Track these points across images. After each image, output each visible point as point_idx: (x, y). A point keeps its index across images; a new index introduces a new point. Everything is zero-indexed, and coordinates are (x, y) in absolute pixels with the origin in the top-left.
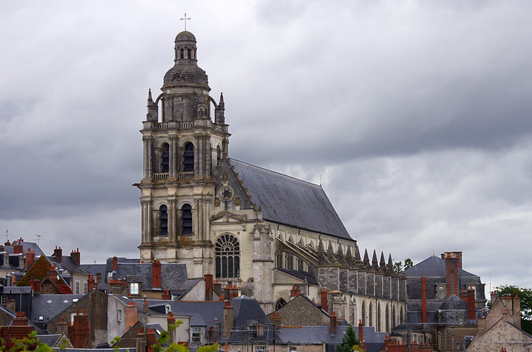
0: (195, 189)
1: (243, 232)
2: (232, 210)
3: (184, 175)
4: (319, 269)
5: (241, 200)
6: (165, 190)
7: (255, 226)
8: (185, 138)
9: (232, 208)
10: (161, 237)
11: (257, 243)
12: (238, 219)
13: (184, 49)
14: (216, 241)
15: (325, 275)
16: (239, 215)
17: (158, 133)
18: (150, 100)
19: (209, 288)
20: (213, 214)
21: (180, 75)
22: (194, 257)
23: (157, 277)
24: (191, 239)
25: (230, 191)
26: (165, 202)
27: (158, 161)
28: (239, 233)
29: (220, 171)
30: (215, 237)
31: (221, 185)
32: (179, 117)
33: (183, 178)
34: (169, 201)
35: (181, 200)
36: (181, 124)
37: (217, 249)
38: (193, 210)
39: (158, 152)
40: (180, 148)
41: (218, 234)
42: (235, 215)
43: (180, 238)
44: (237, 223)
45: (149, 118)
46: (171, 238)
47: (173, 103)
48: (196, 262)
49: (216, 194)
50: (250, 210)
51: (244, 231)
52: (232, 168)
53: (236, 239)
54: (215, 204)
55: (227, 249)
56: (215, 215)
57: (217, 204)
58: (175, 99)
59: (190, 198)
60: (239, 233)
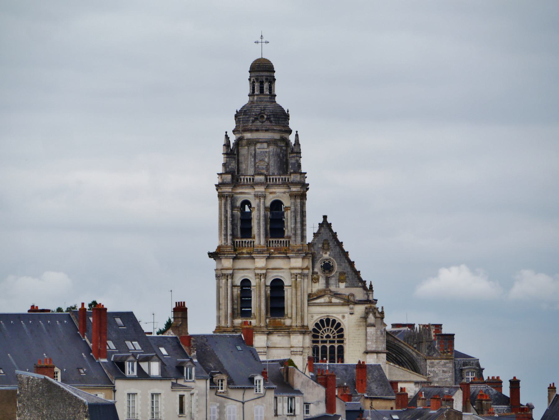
0: (292, 260)
1: (350, 315)
2: (335, 288)
4: (428, 362)
5: (346, 275)
6: (252, 260)
7: (366, 308)
8: (274, 195)
9: (335, 286)
10: (244, 319)
12: (344, 299)
13: (264, 82)
14: (314, 326)
15: (436, 369)
16: (344, 294)
17: (238, 188)
18: (227, 145)
19: (467, 399)
20: (310, 292)
21: (264, 115)
22: (292, 346)
23: (362, 381)
24: (284, 324)
25: (331, 264)
26: (250, 276)
27: (237, 223)
28: (343, 317)
30: (313, 321)
31: (319, 256)
32: (263, 169)
34: (256, 275)
35: (270, 274)
36: (268, 178)
37: (314, 336)
38: (287, 286)
39: (236, 211)
40: (267, 208)
41: (317, 318)
42: (340, 294)
43: (270, 321)
44: (343, 305)
45: (226, 169)
46: (260, 321)
47: (255, 150)
48: (295, 353)
49: (313, 268)
50: (358, 289)
51: (351, 314)
52: (334, 235)
53: (339, 324)
54: (312, 280)
55: (328, 336)
56: (313, 293)
57: (315, 280)
58: (259, 145)
59: (283, 272)
60: (343, 317)
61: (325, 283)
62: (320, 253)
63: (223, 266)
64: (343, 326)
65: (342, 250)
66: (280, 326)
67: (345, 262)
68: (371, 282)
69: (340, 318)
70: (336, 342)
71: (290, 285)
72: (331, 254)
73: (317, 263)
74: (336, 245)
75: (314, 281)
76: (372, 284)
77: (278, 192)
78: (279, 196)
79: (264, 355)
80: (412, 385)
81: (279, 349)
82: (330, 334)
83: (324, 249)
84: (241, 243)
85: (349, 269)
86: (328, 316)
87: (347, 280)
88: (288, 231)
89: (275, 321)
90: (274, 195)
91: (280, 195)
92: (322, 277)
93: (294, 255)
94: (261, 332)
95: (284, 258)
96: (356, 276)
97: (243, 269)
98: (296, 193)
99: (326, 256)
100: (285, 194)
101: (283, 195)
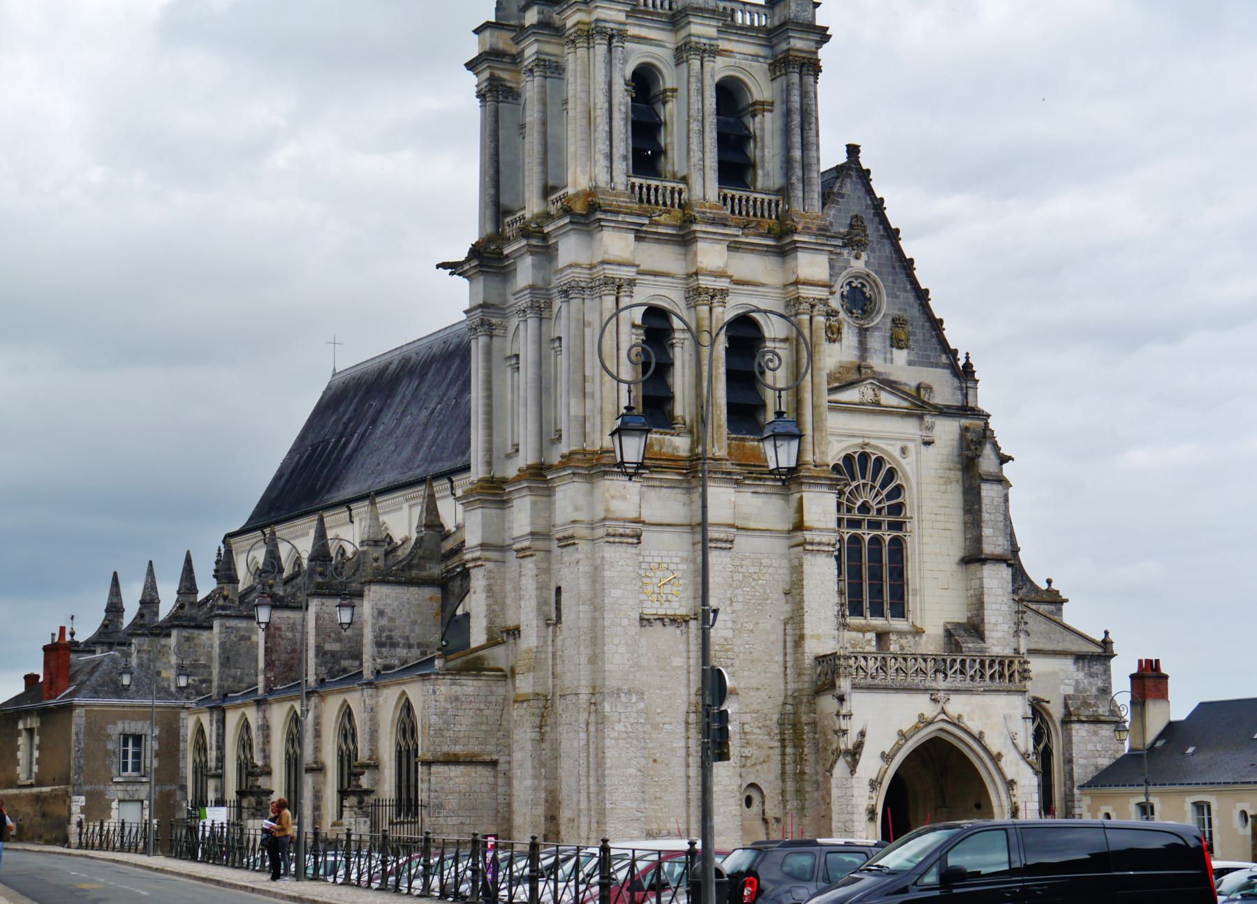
1: (923, 448)
2: (882, 362)
3: (737, 201)
9: (882, 356)
11: (993, 494)
25: (867, 291)
26: (670, 296)
29: (839, 211)
31: (842, 264)
33: (740, 213)
38: (774, 340)
48: (815, 548)
50: (939, 370)
51: (928, 443)
52: (878, 205)
53: (891, 474)
55: (865, 508)
60: (904, 451)
61: (856, 345)
63: (606, 252)
64: (903, 478)
65: (899, 251)
66: (757, 464)
67: (905, 290)
68: (967, 354)
70: (885, 526)
71: (782, 336)
72: (872, 260)
75: (830, 335)
76: (971, 361)
77: (740, 53)
78: (740, 64)
79: (725, 549)
80: (1068, 664)
81: (757, 533)
82: (870, 501)
84: (645, 189)
85: (915, 312)
86: (867, 444)
87: (910, 343)
88: (766, 175)
89: (744, 446)
90: (728, 59)
91: (743, 62)
92: (849, 328)
93: (814, 241)
94: (723, 473)
95: (768, 250)
96: (934, 333)
97: (655, 274)
98: (804, 55)
99: (859, 265)
100: (758, 61)
101: (753, 63)
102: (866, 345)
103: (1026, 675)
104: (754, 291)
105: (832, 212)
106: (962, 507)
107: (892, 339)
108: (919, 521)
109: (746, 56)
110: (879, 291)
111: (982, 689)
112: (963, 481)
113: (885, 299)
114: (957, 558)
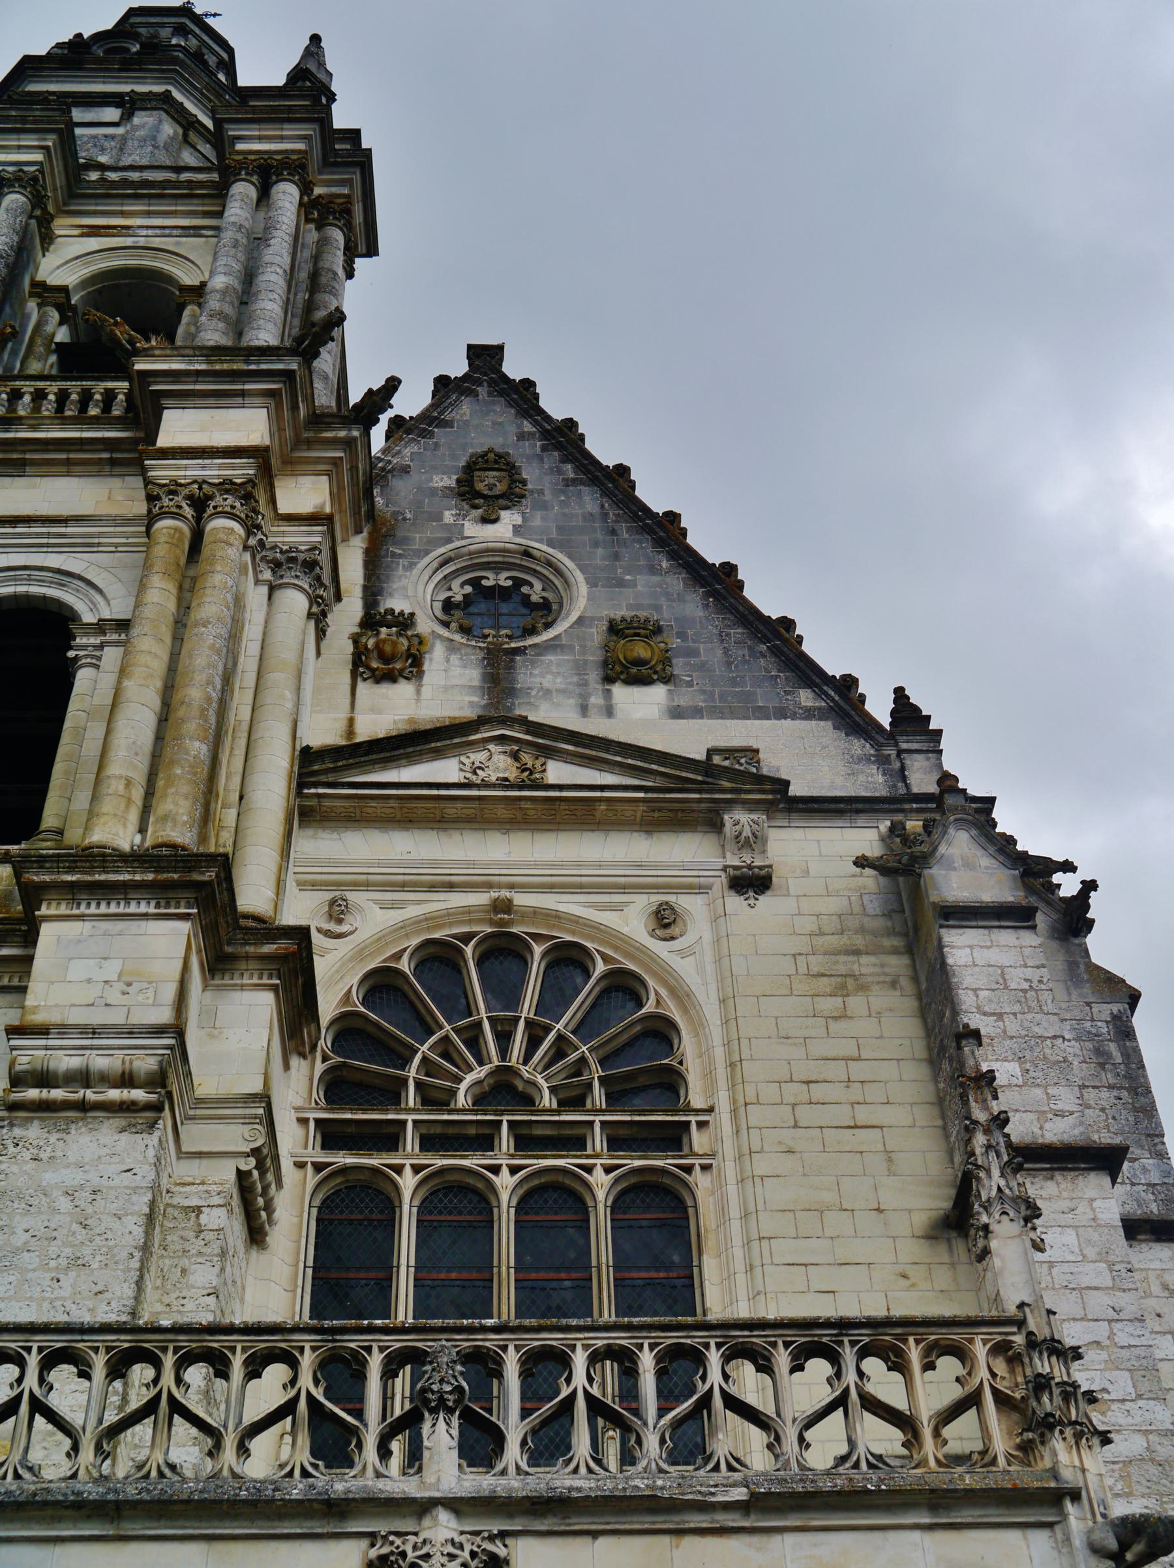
1: (735, 902)
50: (787, 723)
59: (89, 546)
61: (476, 683)
62: (439, 518)
69: (625, 930)
73: (412, 566)
74: (573, 480)
83: (480, 495)
93: (203, 367)
96: (763, 648)
102: (513, 681)
103: (1048, 1404)
104: (49, 535)
105: (407, 451)
106: (923, 1054)
107: (605, 663)
108: (734, 1111)
109: (167, 232)
110: (566, 582)
111: (739, 1494)
112: (915, 979)
113: (583, 589)
114: (921, 1221)
